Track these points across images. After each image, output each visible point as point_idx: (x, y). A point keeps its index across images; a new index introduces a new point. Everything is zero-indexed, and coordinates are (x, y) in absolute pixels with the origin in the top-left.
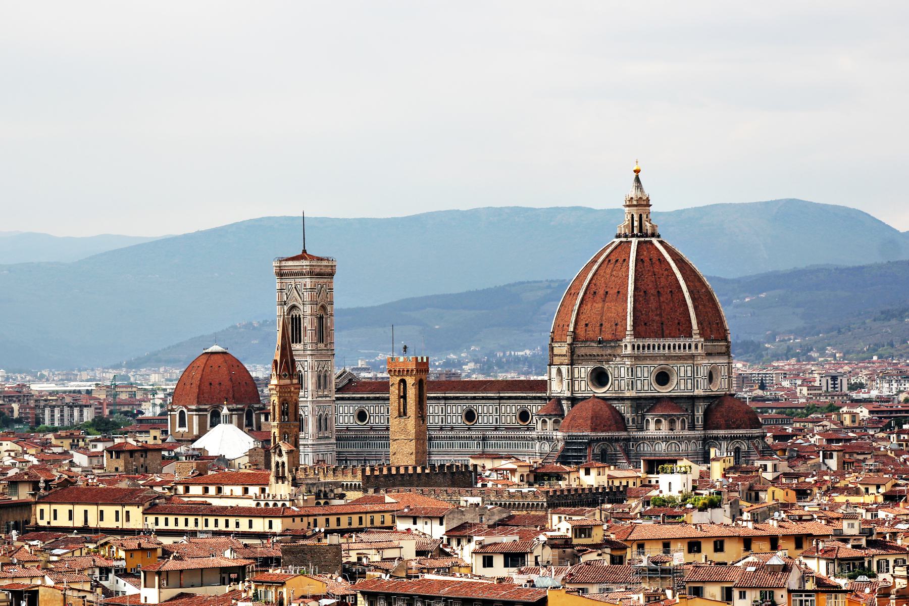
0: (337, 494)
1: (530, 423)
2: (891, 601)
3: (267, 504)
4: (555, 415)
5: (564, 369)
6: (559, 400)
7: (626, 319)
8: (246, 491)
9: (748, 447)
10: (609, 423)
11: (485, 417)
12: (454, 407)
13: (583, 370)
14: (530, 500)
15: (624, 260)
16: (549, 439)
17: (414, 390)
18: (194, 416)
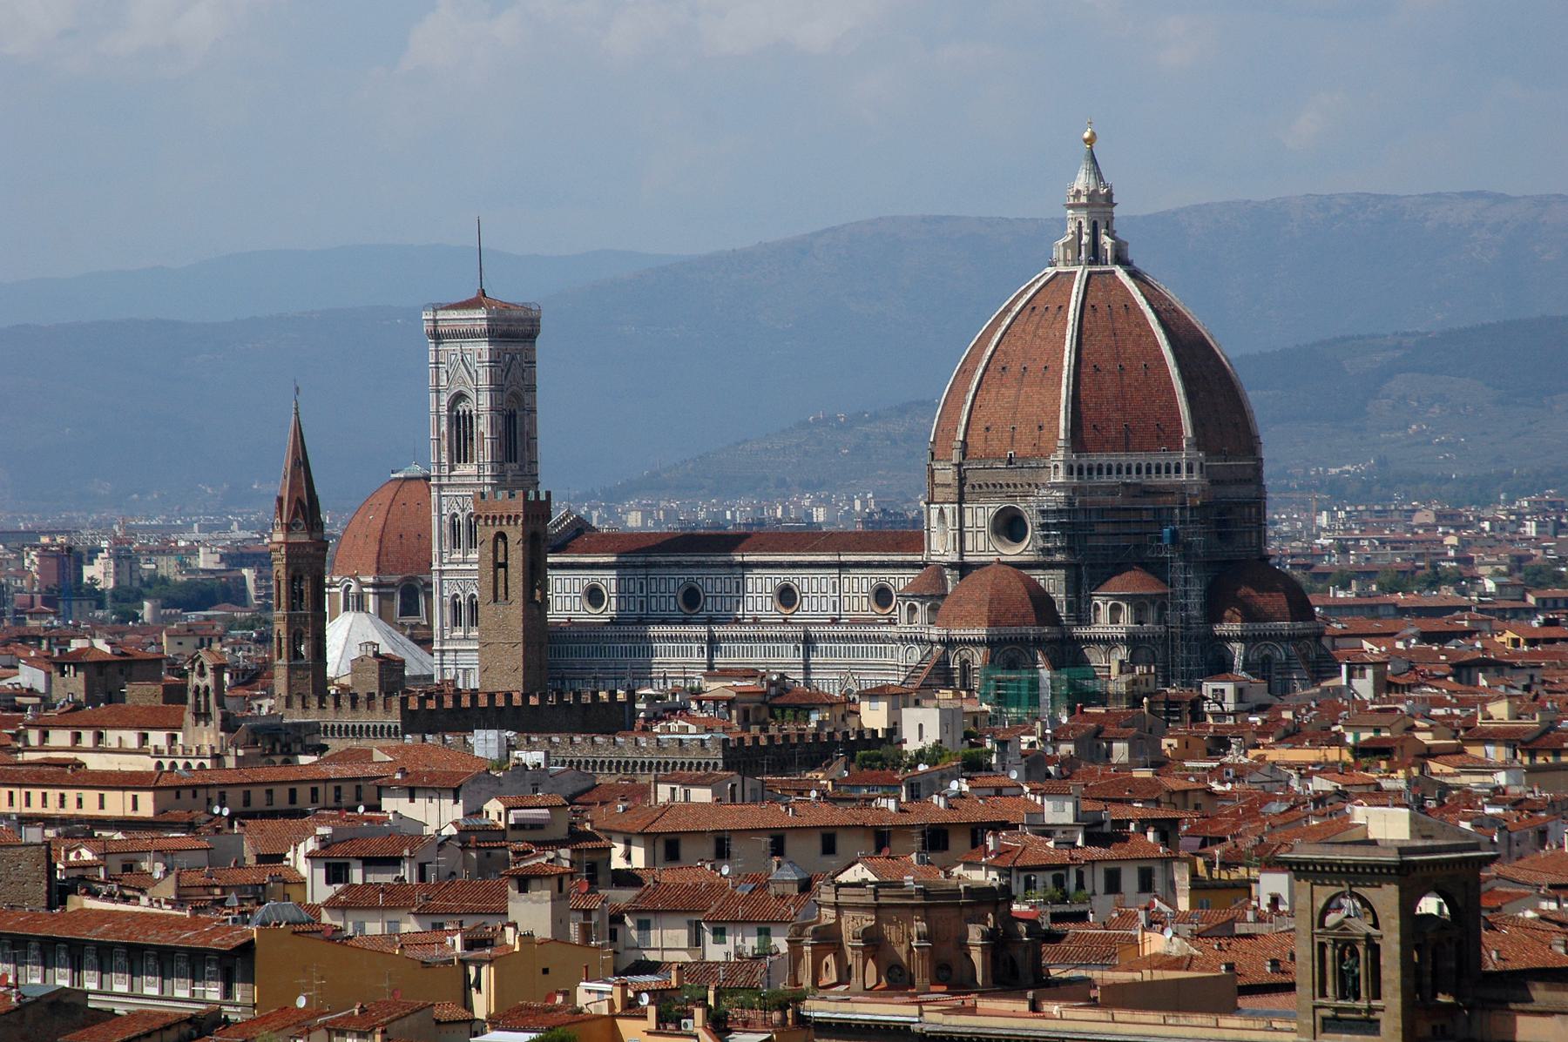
0: (310, 746)
1: (894, 610)
2: (805, 948)
3: (173, 765)
4: (932, 597)
5: (949, 509)
6: (940, 568)
7: (1058, 418)
8: (144, 738)
9: (1287, 655)
10: (1023, 611)
11: (815, 600)
12: (759, 581)
13: (980, 512)
14: (694, 756)
15: (1060, 307)
16: (920, 641)
17: (520, 552)
18: (371, 596)
